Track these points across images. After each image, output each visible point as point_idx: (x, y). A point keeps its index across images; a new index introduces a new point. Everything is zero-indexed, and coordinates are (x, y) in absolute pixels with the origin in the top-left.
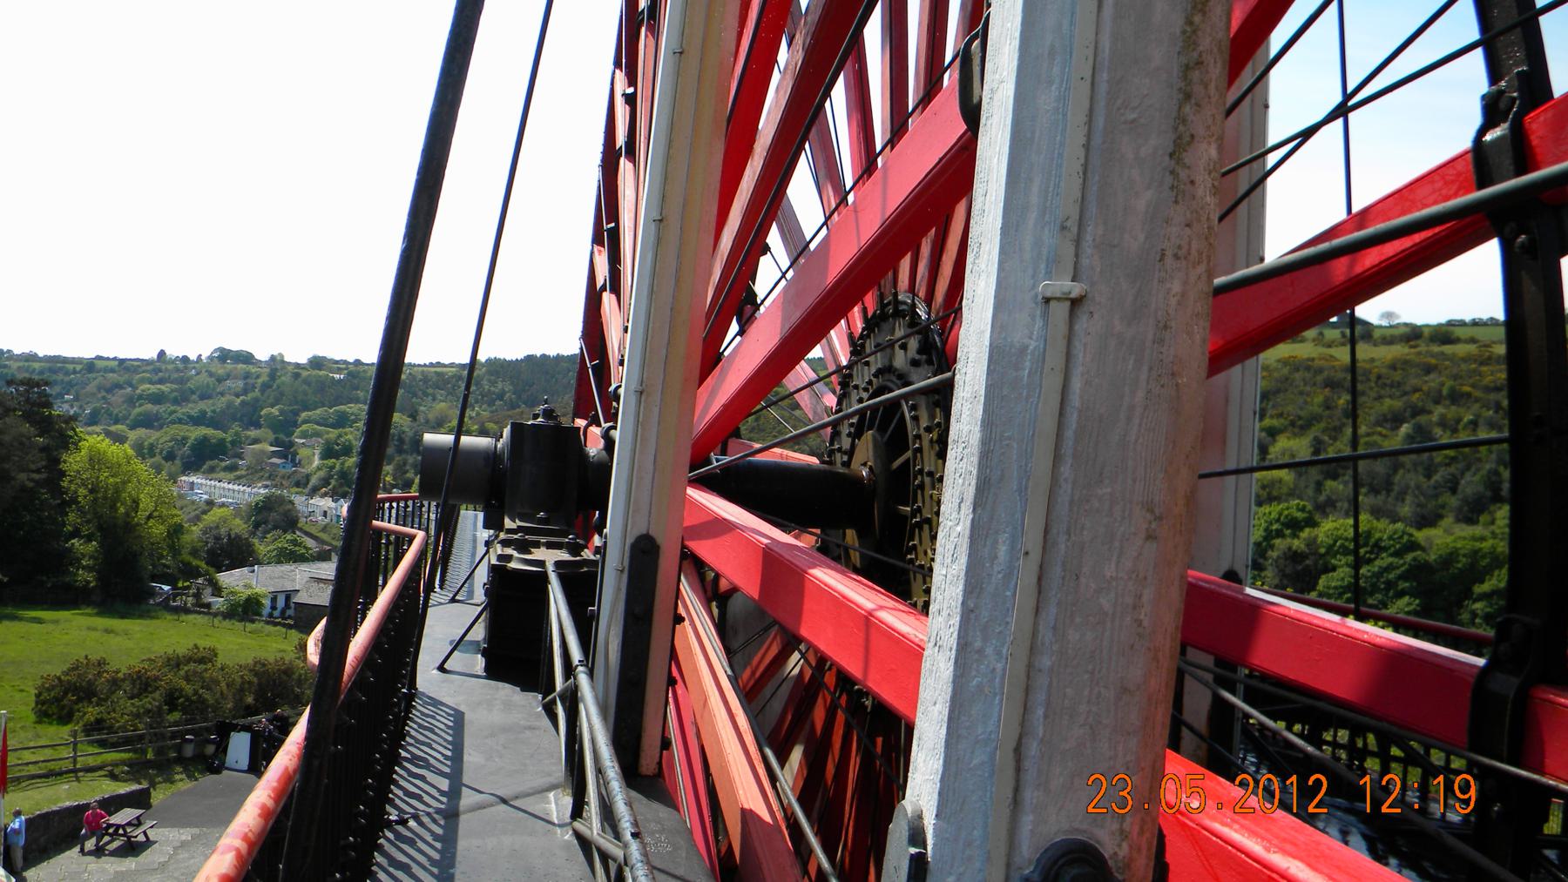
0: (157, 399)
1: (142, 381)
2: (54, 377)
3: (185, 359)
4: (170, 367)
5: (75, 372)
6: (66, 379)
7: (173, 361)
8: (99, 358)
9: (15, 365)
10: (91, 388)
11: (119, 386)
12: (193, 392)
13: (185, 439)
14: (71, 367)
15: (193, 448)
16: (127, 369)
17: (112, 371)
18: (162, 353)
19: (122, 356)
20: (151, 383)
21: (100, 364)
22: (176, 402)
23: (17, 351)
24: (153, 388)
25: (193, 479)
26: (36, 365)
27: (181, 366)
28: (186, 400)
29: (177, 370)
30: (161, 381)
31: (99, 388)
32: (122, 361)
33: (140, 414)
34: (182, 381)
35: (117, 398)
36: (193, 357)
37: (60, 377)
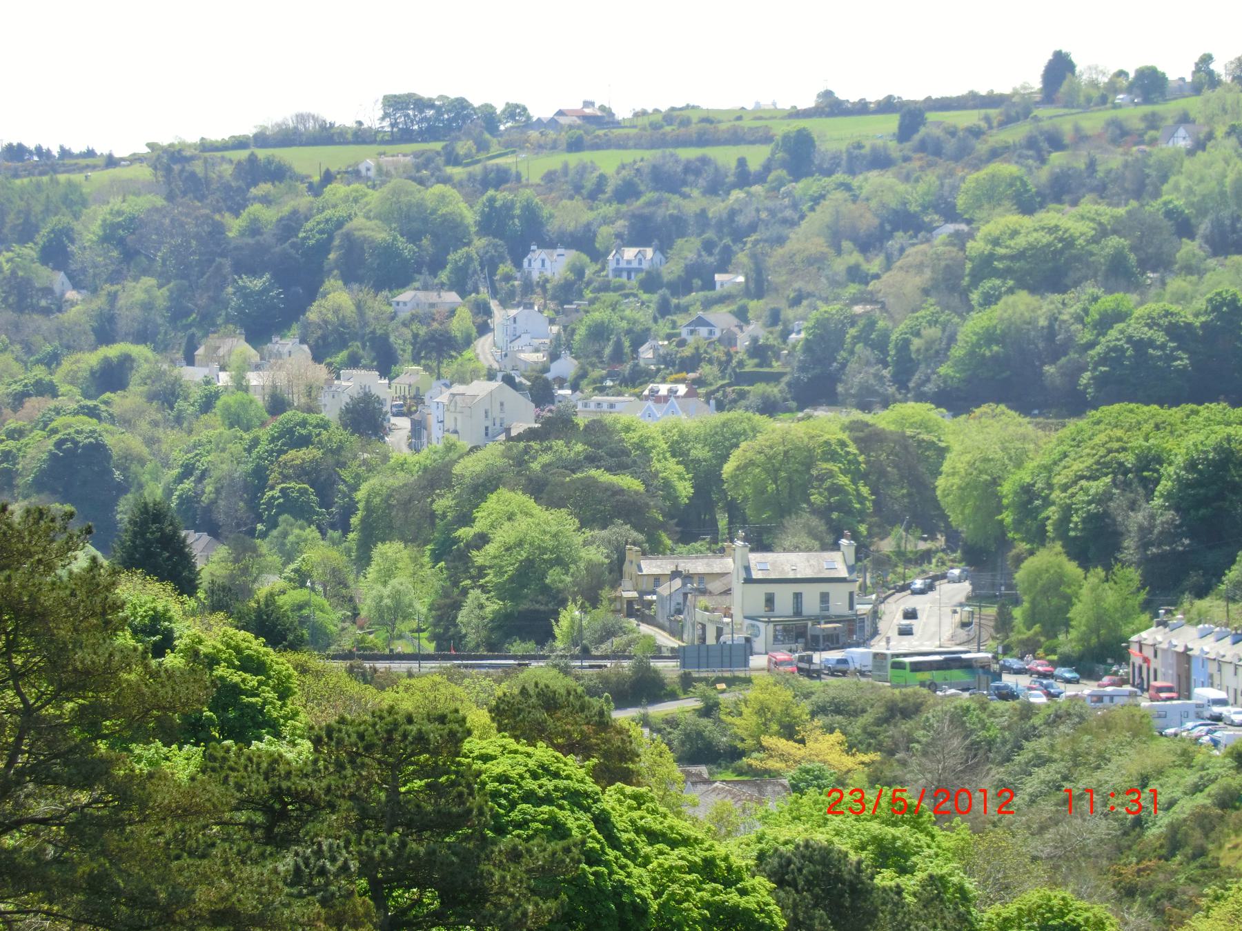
0: (1050, 270)
1: (990, 195)
2: (674, 204)
3: (1150, 84)
4: (1093, 122)
5: (744, 178)
6: (717, 208)
7: (1104, 97)
8: (831, 107)
9: (533, 167)
10: (806, 238)
11: (906, 222)
12: (1185, 228)
13: (1150, 462)
14: (725, 157)
15: (1182, 500)
16: (931, 149)
17: (880, 161)
18: (1060, 67)
19: (913, 92)
20: (1027, 206)
21: (834, 136)
22: (1119, 273)
23: (541, 110)
24: (1031, 229)
25: (1187, 637)
26: (608, 163)
27: (1132, 113)
28: (1162, 263)
29: (1120, 134)
30: (1062, 190)
31: (836, 236)
32: (911, 116)
33: (989, 337)
34: (1142, 184)
35: (902, 278)
36: (1178, 69)
37: (693, 202)
